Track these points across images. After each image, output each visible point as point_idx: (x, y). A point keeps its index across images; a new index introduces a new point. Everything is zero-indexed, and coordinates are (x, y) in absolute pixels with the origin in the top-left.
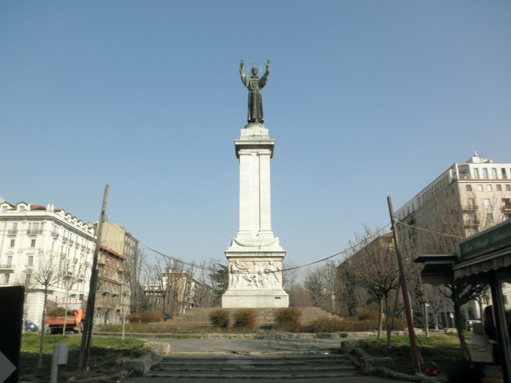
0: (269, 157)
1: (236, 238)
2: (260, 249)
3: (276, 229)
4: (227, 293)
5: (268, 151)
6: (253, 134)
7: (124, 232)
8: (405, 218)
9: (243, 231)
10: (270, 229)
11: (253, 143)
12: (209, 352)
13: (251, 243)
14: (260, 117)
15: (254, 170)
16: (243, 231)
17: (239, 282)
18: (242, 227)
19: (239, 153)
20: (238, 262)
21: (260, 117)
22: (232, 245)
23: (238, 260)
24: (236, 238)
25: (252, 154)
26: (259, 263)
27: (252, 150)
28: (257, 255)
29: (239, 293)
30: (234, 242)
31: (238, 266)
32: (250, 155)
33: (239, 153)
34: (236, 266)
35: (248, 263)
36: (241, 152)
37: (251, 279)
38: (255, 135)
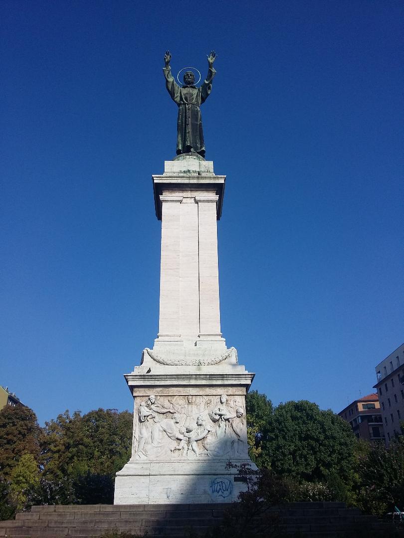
0: (214, 206)
1: (152, 349)
2: (199, 369)
3: (231, 330)
4: (128, 468)
5: (213, 196)
6: (186, 170)
7: (7, 394)
8: (394, 373)
9: (167, 336)
10: (218, 331)
11: (186, 181)
12: (201, 117)
13: (182, 358)
14: (199, 146)
15: (189, 232)
16: (167, 336)
17: (155, 444)
18: (164, 327)
19: (161, 198)
20: (152, 397)
21: (199, 146)
22: (142, 363)
23: (152, 393)
24: (152, 349)
25: (184, 200)
26: (198, 399)
27: (185, 194)
28: (193, 382)
29: (155, 469)
30: (146, 357)
31: (152, 406)
32: (181, 202)
33: (161, 198)
34: (148, 406)
35: (174, 400)
36: (165, 196)
37: (181, 437)
38: (189, 171)
